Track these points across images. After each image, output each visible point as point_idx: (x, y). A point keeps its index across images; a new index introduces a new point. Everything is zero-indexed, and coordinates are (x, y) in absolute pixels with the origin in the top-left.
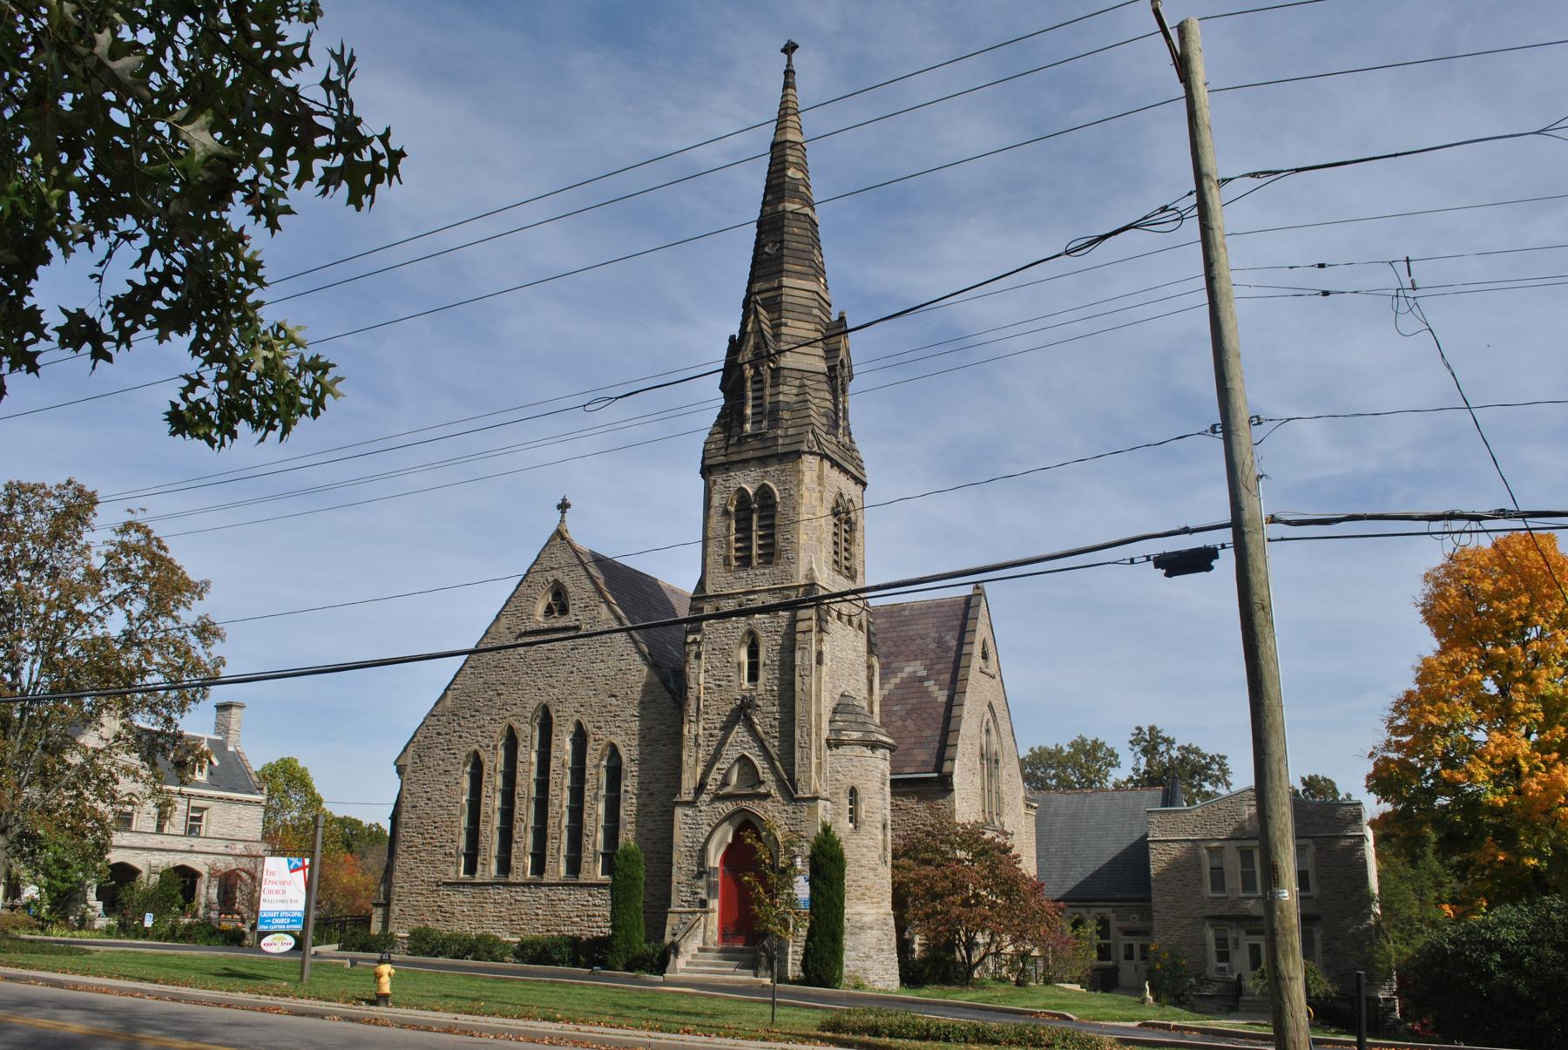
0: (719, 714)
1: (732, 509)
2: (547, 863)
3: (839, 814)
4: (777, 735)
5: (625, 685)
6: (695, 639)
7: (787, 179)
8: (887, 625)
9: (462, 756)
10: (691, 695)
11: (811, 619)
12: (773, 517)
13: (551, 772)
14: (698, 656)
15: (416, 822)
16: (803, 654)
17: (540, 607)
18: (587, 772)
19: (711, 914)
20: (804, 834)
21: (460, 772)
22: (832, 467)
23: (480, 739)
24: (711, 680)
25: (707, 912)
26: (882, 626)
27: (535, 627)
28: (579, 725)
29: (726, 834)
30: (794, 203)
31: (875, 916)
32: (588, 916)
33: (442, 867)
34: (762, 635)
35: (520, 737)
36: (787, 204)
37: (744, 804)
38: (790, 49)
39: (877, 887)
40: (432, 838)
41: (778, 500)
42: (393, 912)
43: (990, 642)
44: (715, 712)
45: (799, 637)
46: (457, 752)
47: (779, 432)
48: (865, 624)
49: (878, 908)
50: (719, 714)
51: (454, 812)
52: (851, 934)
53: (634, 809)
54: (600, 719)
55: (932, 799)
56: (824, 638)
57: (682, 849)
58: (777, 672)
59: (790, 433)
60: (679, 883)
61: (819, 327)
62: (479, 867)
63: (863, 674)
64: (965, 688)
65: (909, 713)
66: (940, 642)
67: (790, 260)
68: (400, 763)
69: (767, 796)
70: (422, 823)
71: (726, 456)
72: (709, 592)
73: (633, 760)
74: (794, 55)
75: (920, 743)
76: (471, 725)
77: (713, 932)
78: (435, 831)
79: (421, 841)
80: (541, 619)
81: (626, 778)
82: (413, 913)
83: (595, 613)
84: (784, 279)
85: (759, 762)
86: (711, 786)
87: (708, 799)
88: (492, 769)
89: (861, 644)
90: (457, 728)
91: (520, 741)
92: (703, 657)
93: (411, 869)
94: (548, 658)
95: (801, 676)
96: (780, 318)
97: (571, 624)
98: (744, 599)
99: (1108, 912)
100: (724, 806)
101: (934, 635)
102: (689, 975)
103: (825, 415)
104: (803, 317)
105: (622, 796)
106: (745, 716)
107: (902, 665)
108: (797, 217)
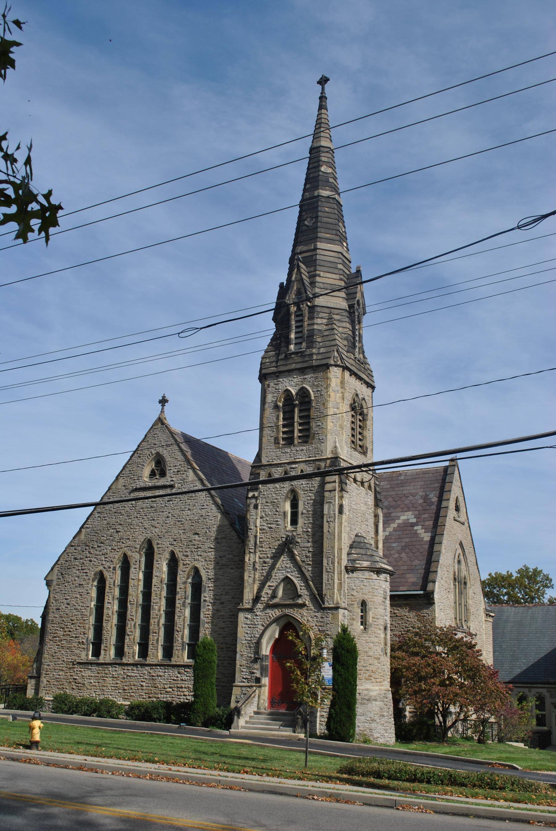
0: (270, 548)
1: (281, 404)
2: (150, 650)
3: (353, 619)
4: (311, 563)
5: (205, 527)
6: (254, 495)
7: (321, 173)
8: (389, 486)
9: (91, 574)
10: (251, 534)
11: (335, 482)
12: (309, 410)
13: (153, 586)
14: (256, 507)
15: (59, 620)
16: (329, 507)
17: (147, 472)
18: (178, 587)
19: (263, 688)
20: (329, 633)
21: (90, 586)
22: (351, 375)
23: (104, 562)
24: (265, 524)
25: (260, 687)
26: (385, 487)
27: (143, 485)
28: (172, 554)
29: (274, 632)
30: (326, 190)
31: (378, 692)
32: (178, 687)
33: (77, 652)
34: (300, 492)
35: (132, 562)
36: (321, 191)
37: (287, 611)
38: (323, 81)
39: (380, 671)
40: (70, 631)
41: (313, 398)
42: (43, 682)
43: (461, 499)
44: (268, 546)
45: (326, 494)
46: (88, 571)
47: (314, 351)
48: (373, 485)
49: (380, 686)
50: (270, 548)
51: (86, 613)
52: (361, 704)
53: (210, 613)
54: (188, 550)
55: (419, 609)
56: (344, 495)
57: (243, 642)
58: (311, 519)
59: (321, 351)
60: (241, 666)
61: (342, 277)
62: (102, 652)
63: (371, 521)
64: (443, 531)
65: (403, 548)
66: (426, 498)
67: (323, 230)
68: (49, 578)
69: (303, 606)
70: (63, 621)
71: (276, 367)
72: (264, 462)
73: (210, 579)
74: (326, 86)
75: (411, 570)
76: (98, 553)
77: (264, 700)
78: (72, 626)
79: (62, 633)
80: (147, 480)
81: (205, 592)
82: (56, 683)
83: (184, 476)
84: (318, 243)
85: (297, 582)
86: (264, 598)
87: (262, 607)
88: (112, 583)
89: (371, 500)
90: (88, 555)
91: (132, 565)
92: (259, 507)
93: (55, 653)
94: (152, 507)
95: (328, 522)
96: (315, 270)
97: (168, 484)
98: (288, 467)
99: (544, 691)
100: (273, 612)
101: (422, 494)
102: (247, 731)
103: (346, 339)
104: (331, 270)
105: (202, 604)
106: (288, 549)
107: (399, 514)
108: (328, 200)
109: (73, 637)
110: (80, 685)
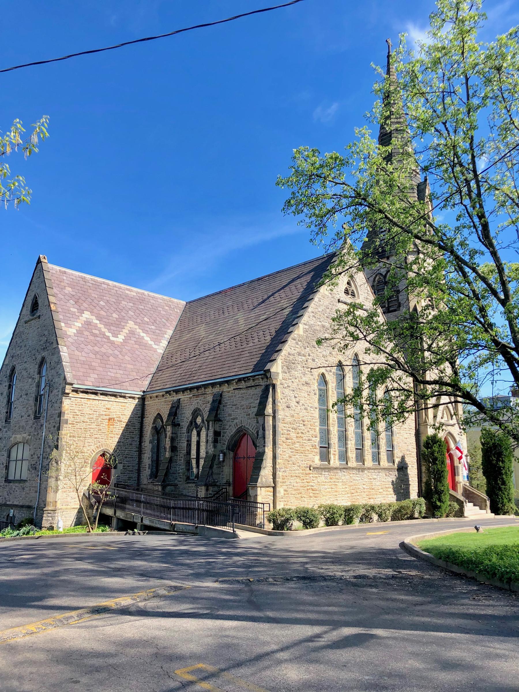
32: (386, 488)
51: (315, 415)
82: (294, 493)
93: (290, 457)
109: (305, 440)
110: (318, 492)
